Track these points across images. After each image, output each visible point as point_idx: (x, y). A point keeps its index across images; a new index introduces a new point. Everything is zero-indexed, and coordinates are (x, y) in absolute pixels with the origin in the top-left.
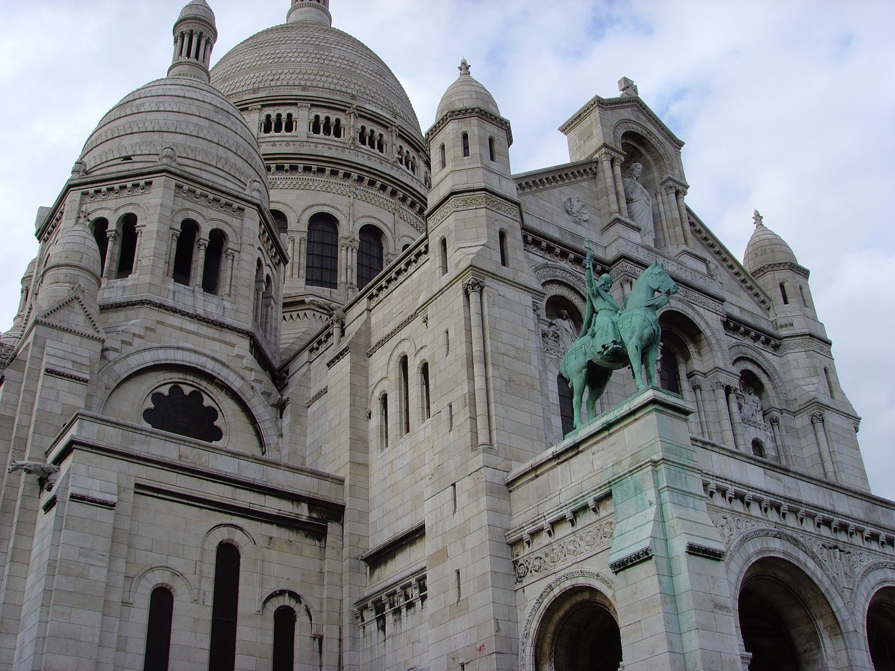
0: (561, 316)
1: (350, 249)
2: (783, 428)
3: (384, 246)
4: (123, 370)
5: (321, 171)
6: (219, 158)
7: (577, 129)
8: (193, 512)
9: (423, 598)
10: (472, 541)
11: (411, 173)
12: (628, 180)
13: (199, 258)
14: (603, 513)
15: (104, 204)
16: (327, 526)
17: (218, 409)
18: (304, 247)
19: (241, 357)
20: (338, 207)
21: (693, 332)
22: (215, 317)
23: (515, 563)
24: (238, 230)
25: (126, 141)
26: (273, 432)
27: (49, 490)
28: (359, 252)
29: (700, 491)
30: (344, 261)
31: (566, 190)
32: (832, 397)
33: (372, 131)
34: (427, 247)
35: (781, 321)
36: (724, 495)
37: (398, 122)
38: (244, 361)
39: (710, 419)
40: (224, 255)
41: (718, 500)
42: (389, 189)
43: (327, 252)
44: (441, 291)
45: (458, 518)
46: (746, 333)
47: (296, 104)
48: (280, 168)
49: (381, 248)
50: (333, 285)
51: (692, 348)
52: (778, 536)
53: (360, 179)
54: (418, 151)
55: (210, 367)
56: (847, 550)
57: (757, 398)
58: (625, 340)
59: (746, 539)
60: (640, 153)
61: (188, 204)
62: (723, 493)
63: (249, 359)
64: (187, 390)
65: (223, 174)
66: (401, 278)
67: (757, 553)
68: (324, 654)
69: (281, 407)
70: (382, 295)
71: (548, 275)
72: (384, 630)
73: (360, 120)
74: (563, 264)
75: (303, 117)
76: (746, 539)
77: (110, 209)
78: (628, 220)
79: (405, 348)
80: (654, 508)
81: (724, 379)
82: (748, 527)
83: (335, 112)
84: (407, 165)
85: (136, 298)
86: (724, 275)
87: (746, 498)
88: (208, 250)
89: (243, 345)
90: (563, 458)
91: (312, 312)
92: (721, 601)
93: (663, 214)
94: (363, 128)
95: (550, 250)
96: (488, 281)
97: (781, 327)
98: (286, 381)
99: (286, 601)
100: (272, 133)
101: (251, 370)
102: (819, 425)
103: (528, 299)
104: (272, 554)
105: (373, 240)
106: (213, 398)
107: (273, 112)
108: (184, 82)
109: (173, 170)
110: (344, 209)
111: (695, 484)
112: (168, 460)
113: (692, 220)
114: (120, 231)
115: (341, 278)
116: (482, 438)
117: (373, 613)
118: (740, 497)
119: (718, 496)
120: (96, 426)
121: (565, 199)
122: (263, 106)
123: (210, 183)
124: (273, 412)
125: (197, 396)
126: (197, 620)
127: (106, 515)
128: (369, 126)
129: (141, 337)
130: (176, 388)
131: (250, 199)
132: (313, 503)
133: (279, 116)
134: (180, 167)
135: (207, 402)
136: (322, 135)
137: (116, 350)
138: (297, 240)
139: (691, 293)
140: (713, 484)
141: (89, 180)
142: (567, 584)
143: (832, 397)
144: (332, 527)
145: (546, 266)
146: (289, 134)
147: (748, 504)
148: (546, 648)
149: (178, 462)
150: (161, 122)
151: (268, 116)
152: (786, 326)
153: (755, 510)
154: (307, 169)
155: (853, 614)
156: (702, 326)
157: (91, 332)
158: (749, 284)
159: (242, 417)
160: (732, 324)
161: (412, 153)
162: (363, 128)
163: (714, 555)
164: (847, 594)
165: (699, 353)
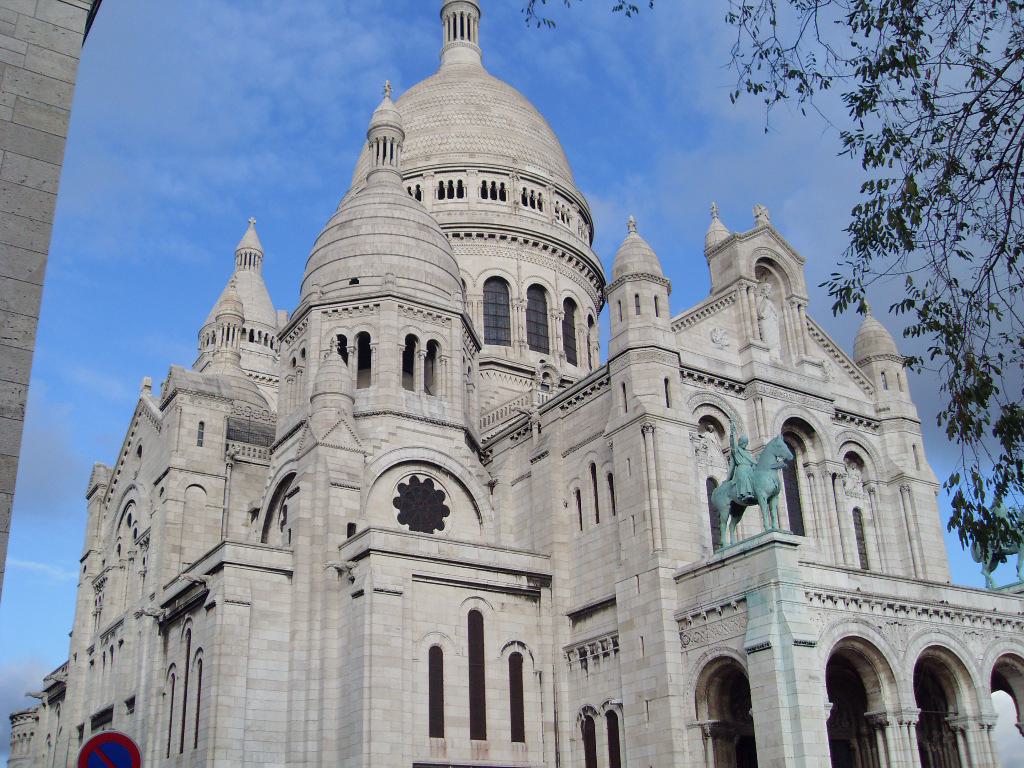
0: (708, 430)
1: (520, 309)
2: (878, 497)
3: (548, 300)
4: (377, 470)
5: (492, 236)
6: (427, 274)
7: (720, 255)
8: (450, 590)
9: (616, 651)
10: (651, 618)
11: (566, 225)
12: (760, 299)
13: (419, 365)
14: (740, 610)
15: (342, 323)
16: (540, 593)
17: (444, 490)
18: (481, 309)
19: (457, 448)
20: (507, 269)
21: (809, 430)
22: (437, 418)
23: (681, 634)
24: (448, 338)
25: (351, 262)
26: (487, 507)
27: (353, 580)
28: (528, 311)
29: (805, 600)
30: (516, 321)
31: (711, 320)
32: (918, 468)
33: (532, 192)
34: (608, 379)
35: (881, 406)
36: (820, 598)
37: (555, 180)
38: (462, 451)
39: (820, 500)
40: (438, 360)
41: (816, 602)
42: (550, 249)
43: (501, 312)
44: (623, 427)
45: (640, 602)
46: (852, 420)
47: (465, 171)
48: (456, 235)
49: (545, 303)
50: (507, 342)
51: (807, 443)
52: (856, 622)
53: (526, 242)
54: (572, 203)
55: (438, 460)
56: (904, 623)
57: (859, 472)
58: (758, 492)
59: (833, 626)
60: (770, 272)
61: (409, 322)
62: (820, 596)
63: (466, 449)
64: (422, 479)
65: (430, 288)
66: (587, 399)
67: (839, 635)
68: (543, 684)
69: (492, 485)
70: (571, 409)
71: (698, 400)
72: (586, 668)
73: (522, 181)
74: (711, 388)
75: (473, 183)
76: (833, 626)
77: (347, 328)
78: (758, 342)
79: (592, 457)
80: (775, 616)
81: (831, 468)
82: (834, 618)
83: (499, 176)
84: (563, 219)
85: (379, 408)
86: (835, 370)
87: (834, 599)
88: (426, 359)
89: (461, 436)
90: (714, 567)
91: (491, 373)
92: (814, 674)
93: (788, 326)
94: (524, 189)
95: (701, 378)
96: (659, 424)
97: (880, 410)
98: (490, 458)
99: (516, 648)
100: (446, 199)
101: (468, 458)
102: (906, 494)
103: (686, 432)
104: (504, 616)
105: (538, 296)
106: (442, 483)
107: (445, 178)
108: (390, 200)
109: (395, 294)
110: (514, 272)
111: (800, 597)
112: (432, 556)
113: (811, 326)
114: (357, 346)
115: (514, 337)
116: (659, 545)
117: (578, 657)
118: (830, 598)
119: (816, 599)
120: (383, 535)
121: (711, 329)
122: (436, 173)
123: (424, 302)
124: (487, 490)
125: (429, 482)
126: (459, 667)
127: (396, 599)
128: (530, 187)
129: (387, 441)
130: (414, 479)
131: (454, 310)
132: (531, 576)
133: (451, 182)
134: (401, 290)
135: (437, 487)
136: (489, 199)
137: (370, 455)
138: (475, 304)
139: (808, 398)
140: (812, 592)
141: (328, 301)
142: (717, 654)
143: (918, 468)
144: (544, 592)
145: (697, 394)
146: (460, 200)
147: (836, 602)
148: (702, 692)
149: (438, 557)
150: (379, 245)
151: (441, 183)
152: (884, 410)
153: (841, 605)
154: (480, 236)
155: (904, 668)
156: (815, 426)
157: (355, 446)
158: (856, 374)
159: (463, 495)
160: (840, 415)
161: (567, 205)
162: (524, 189)
163: (811, 645)
164: (902, 655)
165: (813, 446)
